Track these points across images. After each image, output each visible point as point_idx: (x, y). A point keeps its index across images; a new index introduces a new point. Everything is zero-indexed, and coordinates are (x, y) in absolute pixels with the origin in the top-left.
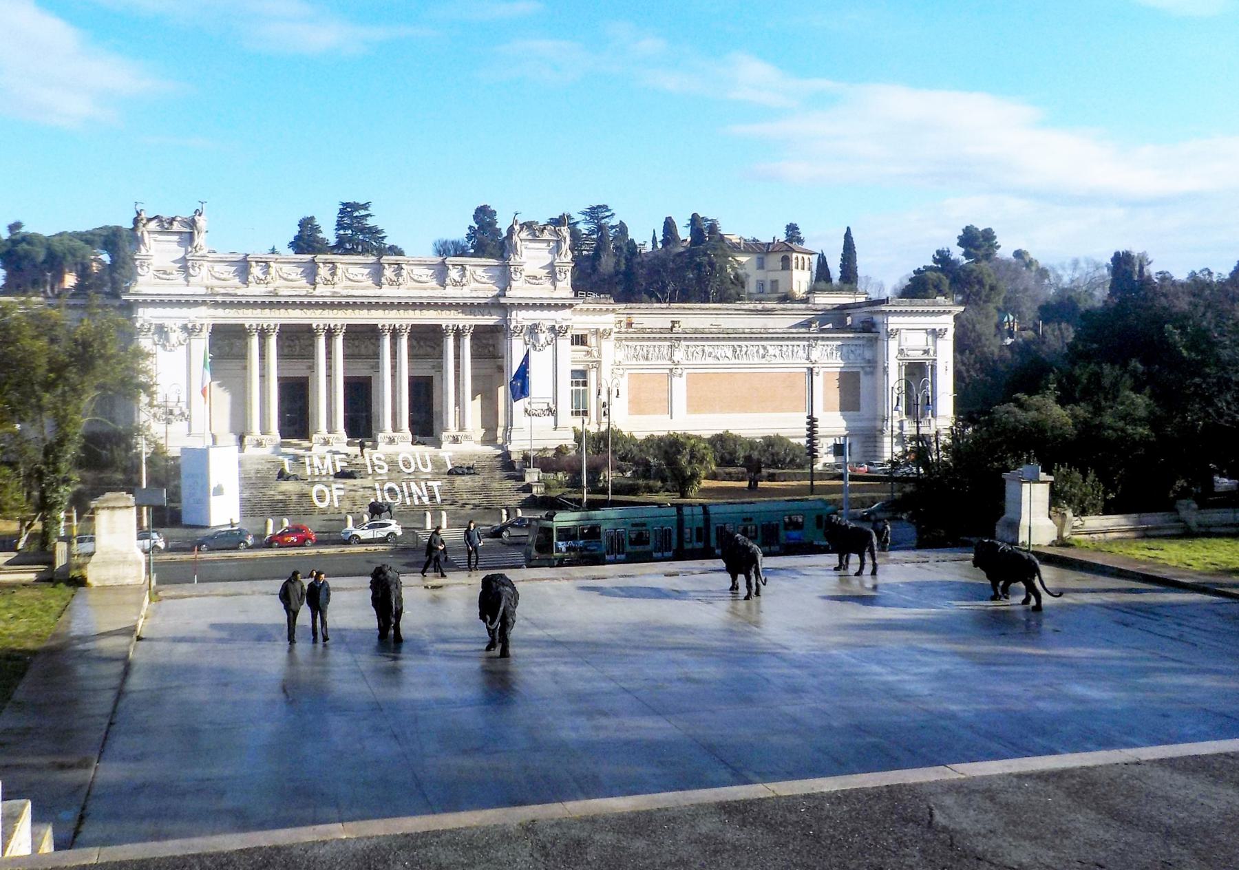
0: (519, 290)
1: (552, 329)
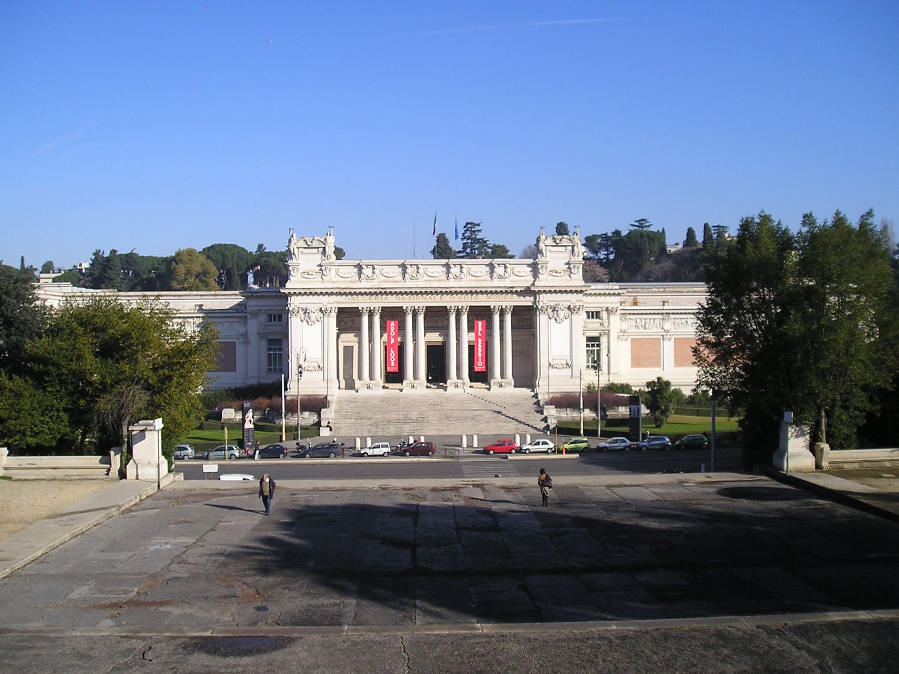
0: (545, 280)
1: (569, 308)
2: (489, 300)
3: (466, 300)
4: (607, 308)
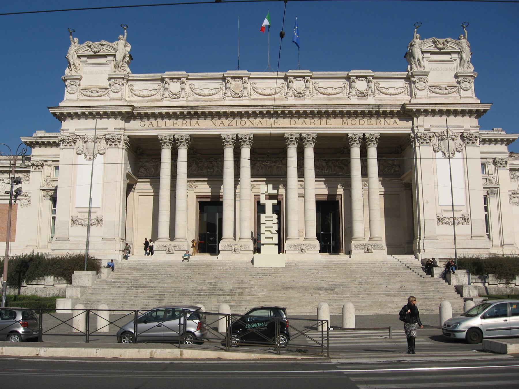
2: (344, 126)
3: (312, 125)
4: (494, 159)
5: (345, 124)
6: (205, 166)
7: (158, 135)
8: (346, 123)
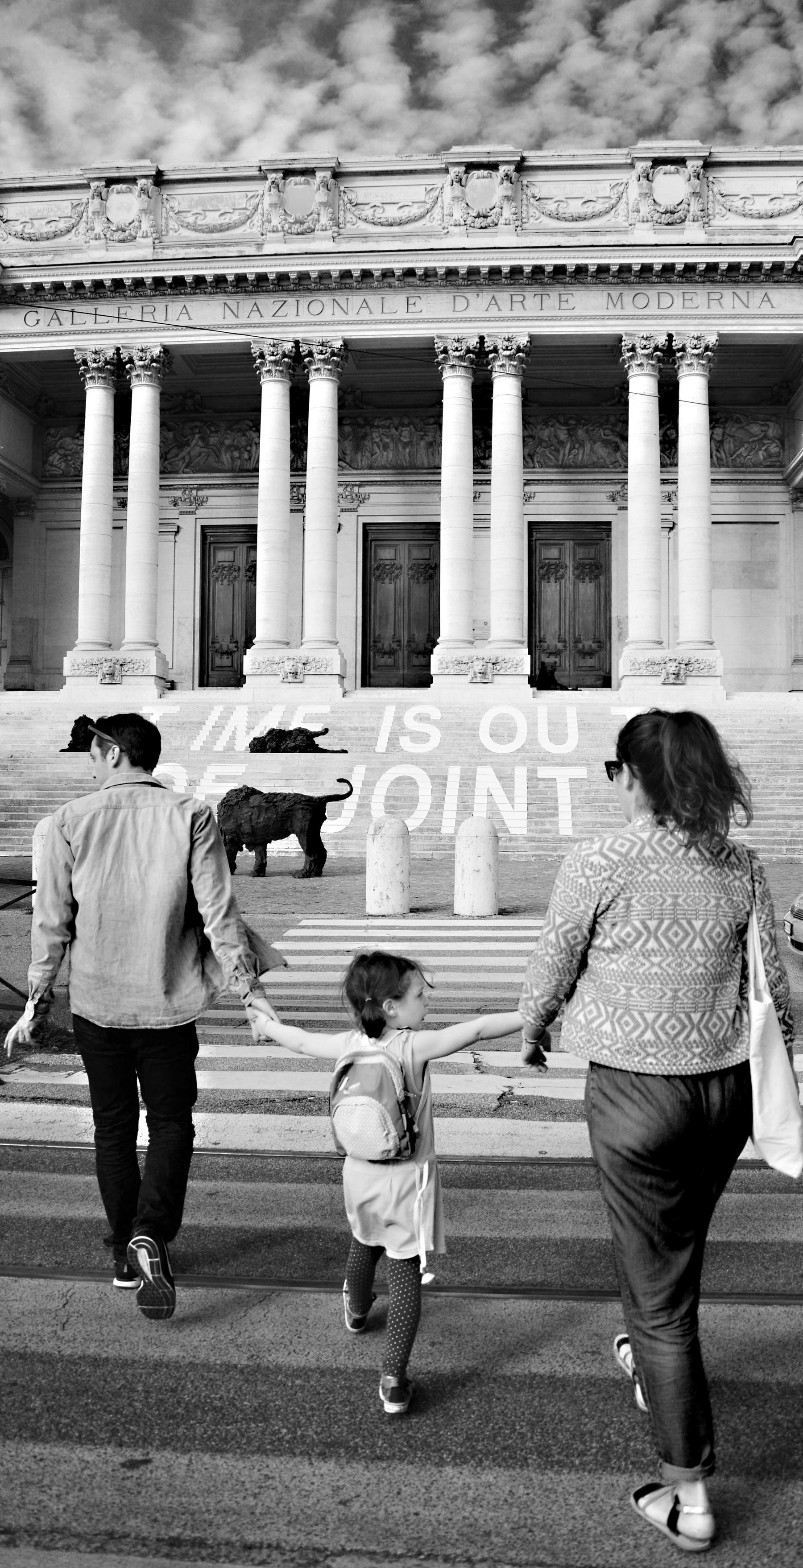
2: (612, 312)
5: (615, 306)
6: (227, 442)
7: (73, 351)
8: (619, 304)
